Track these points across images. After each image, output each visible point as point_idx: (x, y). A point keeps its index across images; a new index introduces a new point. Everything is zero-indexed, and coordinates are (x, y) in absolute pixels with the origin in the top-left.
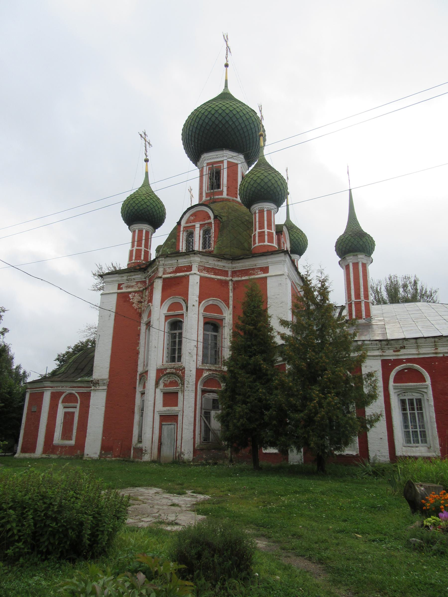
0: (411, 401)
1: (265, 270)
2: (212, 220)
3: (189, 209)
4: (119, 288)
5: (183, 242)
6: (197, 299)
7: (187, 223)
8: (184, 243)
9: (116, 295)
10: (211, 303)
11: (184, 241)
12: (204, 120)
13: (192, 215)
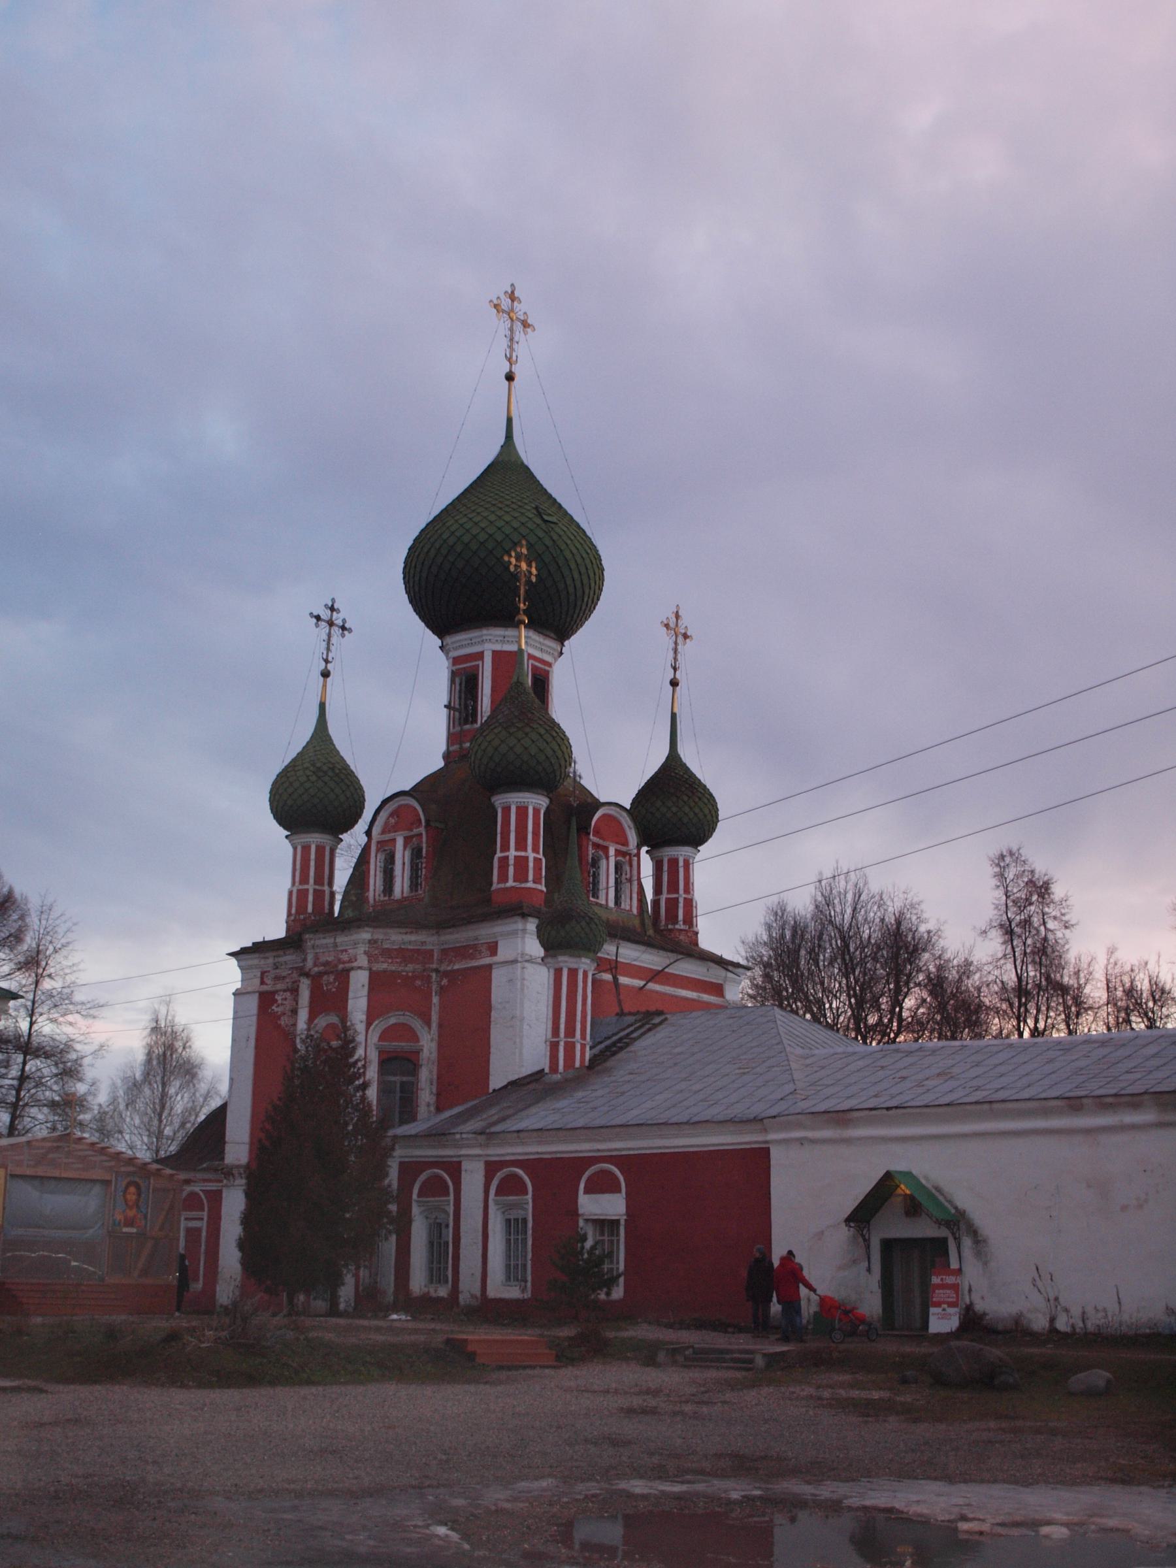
0: (517, 1220)
1: (493, 949)
2: (422, 830)
3: (385, 802)
4: (263, 983)
5: (375, 876)
6: (364, 1017)
7: (383, 832)
8: (378, 878)
9: (257, 995)
10: (392, 1021)
11: (378, 873)
12: (452, 546)
13: (392, 815)
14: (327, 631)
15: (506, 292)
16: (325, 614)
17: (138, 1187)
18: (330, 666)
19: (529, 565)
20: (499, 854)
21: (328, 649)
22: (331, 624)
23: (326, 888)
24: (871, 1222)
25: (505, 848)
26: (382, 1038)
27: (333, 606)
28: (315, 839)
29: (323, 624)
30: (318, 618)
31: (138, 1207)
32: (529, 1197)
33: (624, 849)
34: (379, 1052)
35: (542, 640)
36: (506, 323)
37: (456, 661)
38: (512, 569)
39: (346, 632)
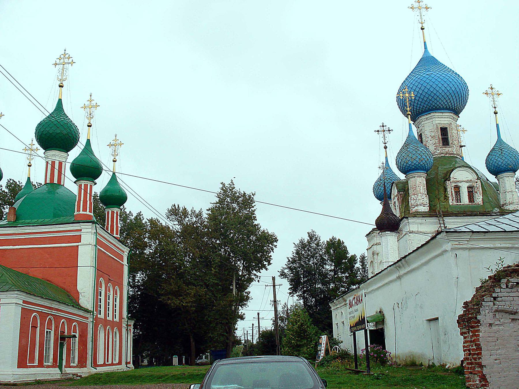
18: (386, 145)
21: (384, 139)
30: (378, 131)
35: (441, 114)
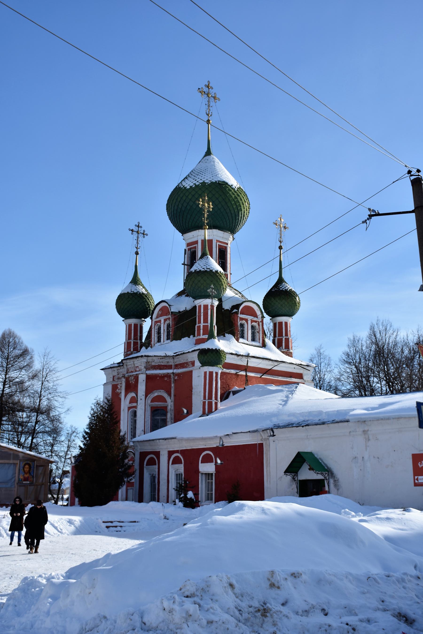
0: (179, 474)
2: (170, 316)
4: (113, 380)
6: (144, 394)
10: (156, 394)
11: (155, 334)
13: (160, 310)
14: (137, 236)
15: (205, 85)
16: (136, 229)
17: (29, 465)
19: (209, 204)
20: (197, 325)
21: (137, 243)
22: (138, 232)
23: (139, 341)
24: (299, 473)
25: (200, 322)
26: (152, 401)
27: (139, 225)
28: (133, 321)
29: (135, 233)
30: (132, 230)
31: (30, 473)
32: (183, 464)
33: (255, 319)
34: (151, 407)
36: (206, 99)
37: (188, 245)
38: (200, 206)
39: (145, 236)
